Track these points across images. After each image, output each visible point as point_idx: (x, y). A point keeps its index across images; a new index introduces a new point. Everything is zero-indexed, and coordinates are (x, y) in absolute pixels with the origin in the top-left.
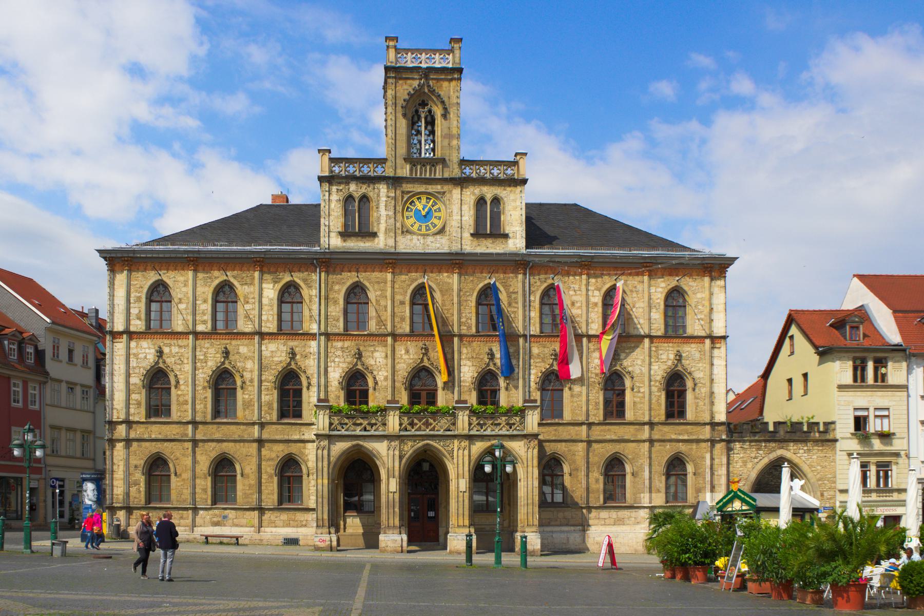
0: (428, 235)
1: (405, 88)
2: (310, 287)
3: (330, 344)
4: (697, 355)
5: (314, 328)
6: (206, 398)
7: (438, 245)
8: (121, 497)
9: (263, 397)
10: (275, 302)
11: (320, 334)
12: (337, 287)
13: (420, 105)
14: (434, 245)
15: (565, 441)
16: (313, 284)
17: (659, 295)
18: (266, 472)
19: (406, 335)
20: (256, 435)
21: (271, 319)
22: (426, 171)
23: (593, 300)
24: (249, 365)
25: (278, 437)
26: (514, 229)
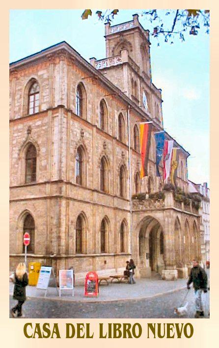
8: (64, 248)
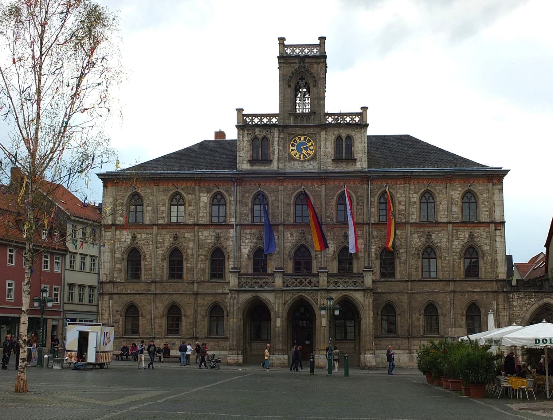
0: (305, 161)
1: (289, 70)
2: (230, 195)
3: (242, 231)
4: (485, 235)
5: (232, 221)
6: (163, 266)
7: (311, 167)
9: (199, 265)
10: (208, 205)
11: (236, 225)
12: (247, 195)
13: (300, 79)
14: (309, 167)
15: (396, 293)
16: (232, 193)
17: (458, 196)
18: (201, 314)
19: (292, 225)
20: (195, 289)
21: (205, 216)
22: (303, 120)
23: (413, 200)
24: (191, 245)
25: (208, 291)
26: (360, 156)
